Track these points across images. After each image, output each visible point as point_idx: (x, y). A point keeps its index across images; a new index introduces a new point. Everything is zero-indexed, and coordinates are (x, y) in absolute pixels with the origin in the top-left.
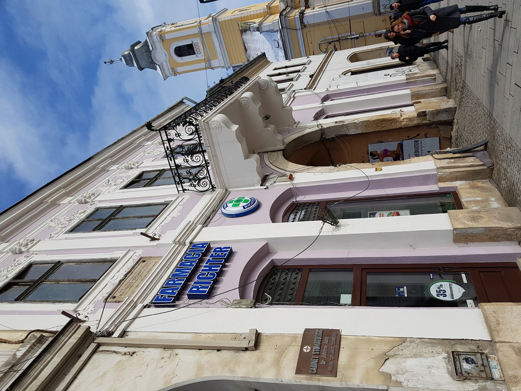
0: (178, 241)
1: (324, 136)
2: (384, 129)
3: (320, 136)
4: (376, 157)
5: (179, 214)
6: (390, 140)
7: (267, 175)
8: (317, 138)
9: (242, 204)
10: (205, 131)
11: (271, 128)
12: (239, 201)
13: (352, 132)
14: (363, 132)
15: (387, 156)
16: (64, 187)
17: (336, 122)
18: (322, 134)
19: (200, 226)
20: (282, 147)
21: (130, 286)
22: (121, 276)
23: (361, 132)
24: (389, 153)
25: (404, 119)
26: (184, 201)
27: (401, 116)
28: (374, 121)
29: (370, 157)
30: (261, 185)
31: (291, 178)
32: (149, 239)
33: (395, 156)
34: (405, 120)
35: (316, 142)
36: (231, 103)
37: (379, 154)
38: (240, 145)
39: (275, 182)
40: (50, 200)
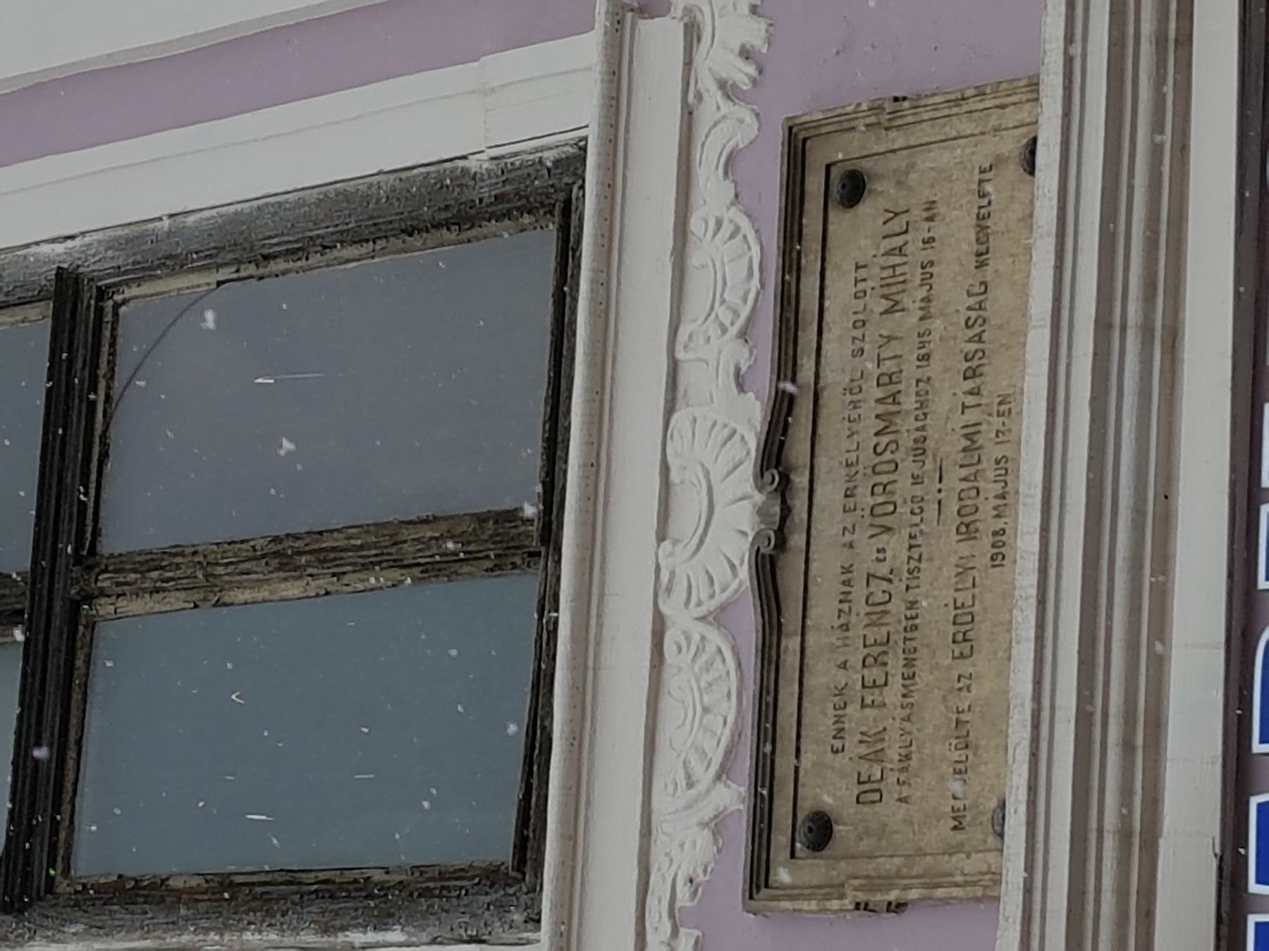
21: (892, 647)
22: (734, 516)
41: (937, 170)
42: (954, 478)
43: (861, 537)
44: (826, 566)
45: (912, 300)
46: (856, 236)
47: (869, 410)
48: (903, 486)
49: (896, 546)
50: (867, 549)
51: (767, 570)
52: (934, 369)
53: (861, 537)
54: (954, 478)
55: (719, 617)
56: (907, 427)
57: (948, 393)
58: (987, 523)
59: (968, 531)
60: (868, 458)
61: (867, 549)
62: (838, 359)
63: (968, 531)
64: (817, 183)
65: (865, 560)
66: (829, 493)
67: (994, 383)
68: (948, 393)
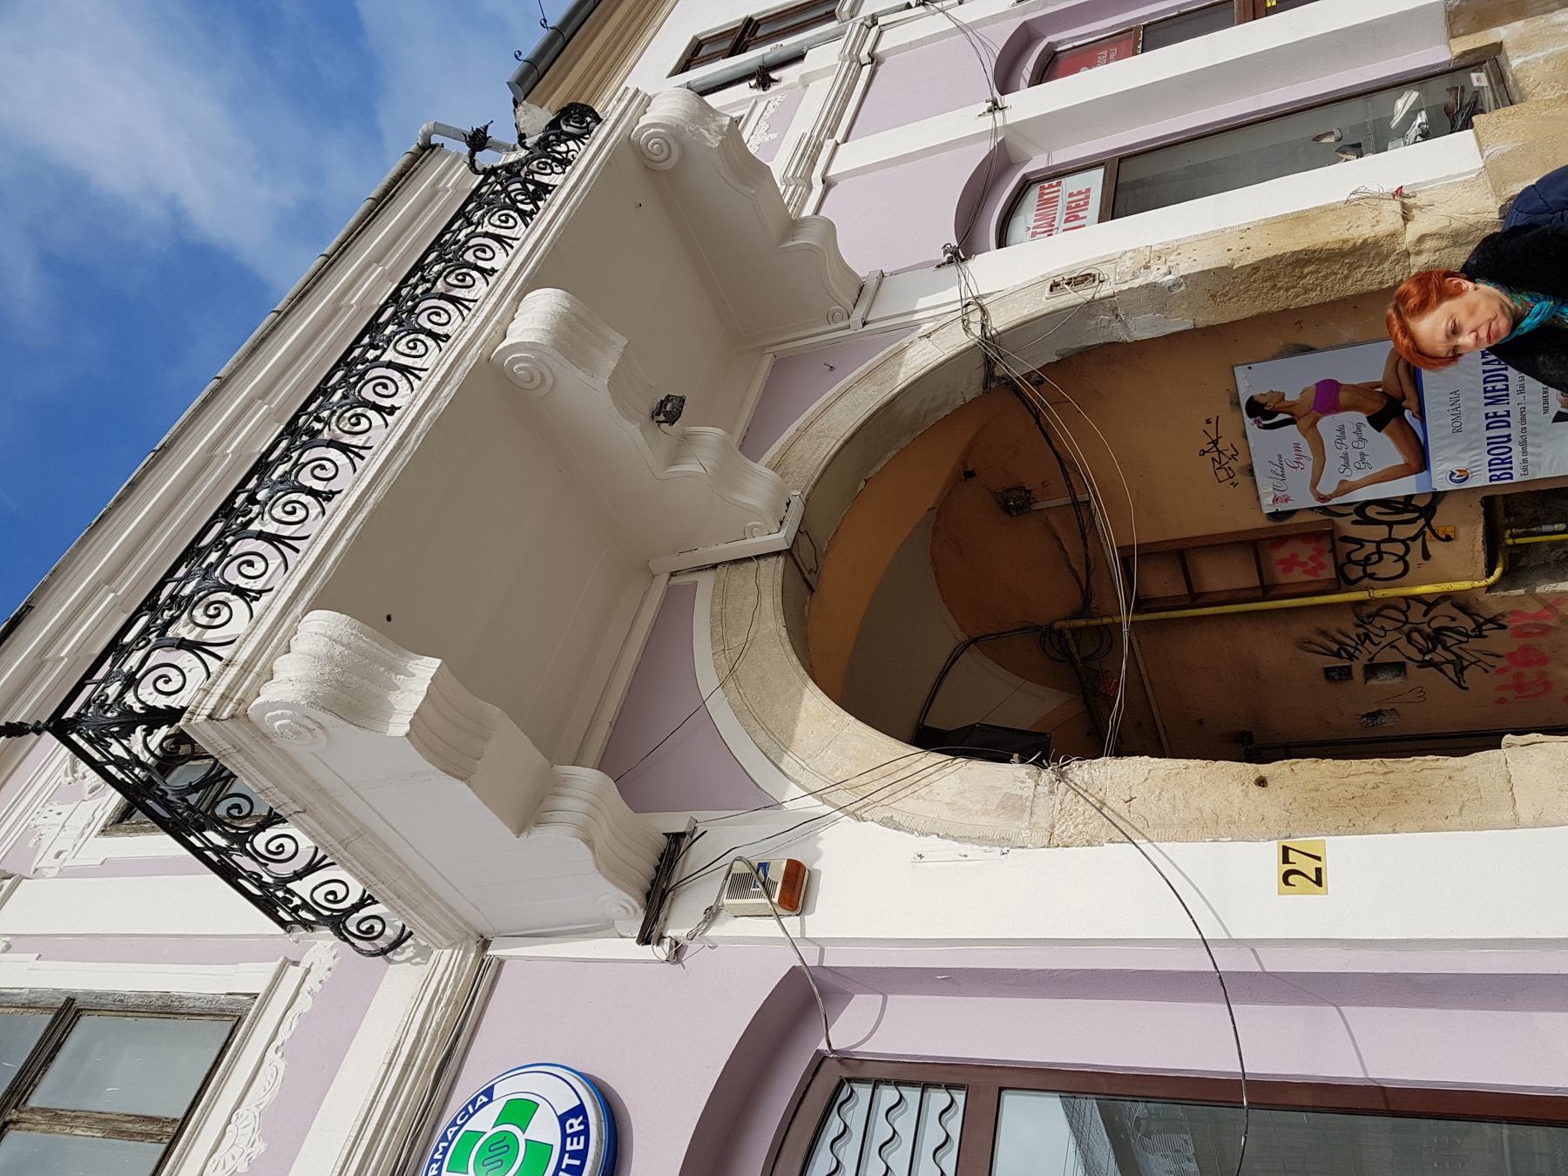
1: (1000, 371)
2: (1314, 297)
3: (979, 375)
4: (1281, 417)
5: (260, 1147)
6: (1347, 334)
7: (683, 834)
8: (970, 386)
13: (1143, 327)
14: (1203, 320)
15: (1335, 408)
18: (989, 363)
20: (779, 539)
23: (1189, 325)
24: (1344, 397)
25: (1421, 239)
26: (304, 1003)
27: (1406, 218)
28: (1255, 268)
29: (1248, 421)
30: (644, 939)
31: (795, 889)
33: (1377, 407)
34: (1429, 244)
35: (966, 406)
37: (1293, 404)
38: (464, 786)
39: (712, 914)
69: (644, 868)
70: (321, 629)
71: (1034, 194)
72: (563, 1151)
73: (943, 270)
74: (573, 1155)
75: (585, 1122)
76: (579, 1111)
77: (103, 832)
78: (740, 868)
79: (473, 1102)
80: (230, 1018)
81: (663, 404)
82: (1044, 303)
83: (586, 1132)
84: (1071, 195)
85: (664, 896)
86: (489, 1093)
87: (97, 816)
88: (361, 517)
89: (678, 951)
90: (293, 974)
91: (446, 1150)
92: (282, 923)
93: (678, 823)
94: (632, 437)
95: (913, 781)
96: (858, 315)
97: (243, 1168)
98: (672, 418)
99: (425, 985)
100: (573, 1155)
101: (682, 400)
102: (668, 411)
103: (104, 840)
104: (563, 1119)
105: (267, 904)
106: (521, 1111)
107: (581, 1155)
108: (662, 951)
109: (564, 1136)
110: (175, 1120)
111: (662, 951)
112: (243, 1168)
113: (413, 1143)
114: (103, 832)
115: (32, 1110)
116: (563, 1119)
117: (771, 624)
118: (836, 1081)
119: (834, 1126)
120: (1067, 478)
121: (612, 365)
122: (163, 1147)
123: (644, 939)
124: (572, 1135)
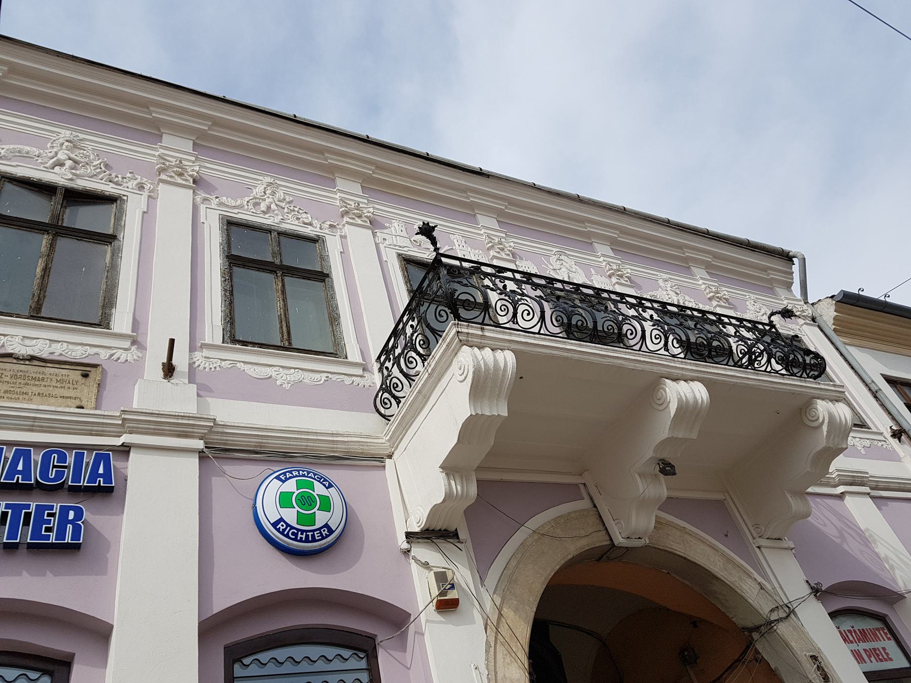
0: (124, 419)
1: (755, 635)
3: (750, 624)
8: (742, 620)
9: (290, 516)
10: (444, 346)
11: (661, 489)
12: (306, 501)
16: (379, 167)
17: (814, 658)
18: (757, 628)
19: (200, 444)
20: (619, 540)
26: (348, 380)
30: (409, 535)
32: (165, 361)
35: (730, 621)
36: (620, 368)
39: (426, 565)
40: (332, 160)
41: (87, 392)
42: (19, 390)
43: (11, 373)
44: (8, 366)
45: (58, 385)
46: (76, 375)
47: (38, 376)
48: (20, 381)
49: (8, 379)
50: (8, 374)
51: (10, 355)
52: (42, 388)
53: (11, 373)
54: (19, 390)
55: (3, 346)
56: (32, 382)
57: (36, 390)
58: (6, 395)
59: (6, 392)
60: (27, 375)
61: (8, 374)
62: (50, 371)
63: (6, 392)
64: (86, 369)
65: (5, 373)
66: (23, 367)
67: (35, 398)
68: (36, 390)
69: (439, 525)
70: (507, 359)
71: (878, 624)
72: (313, 531)
73: (806, 585)
74: (313, 536)
75: (327, 536)
76: (331, 531)
77: (399, 255)
78: (449, 575)
79: (325, 480)
80: (336, 352)
81: (669, 464)
82: (803, 655)
83: (323, 538)
84: (884, 649)
85: (428, 538)
86: (330, 486)
87: (406, 249)
88: (566, 354)
89: (407, 552)
90: (359, 371)
91: (303, 476)
92: (379, 357)
93: (463, 534)
94: (648, 453)
95: (511, 652)
96: (763, 542)
97: (278, 383)
98: (662, 471)
99: (368, 437)
100: (313, 536)
101: (674, 474)
102: (667, 469)
103: (395, 256)
104: (326, 526)
105: (386, 351)
106: (326, 505)
107: (314, 540)
108: (405, 546)
109: (319, 529)
110: (290, 344)
111: (405, 546)
112: (278, 383)
113: (303, 457)
114: (399, 255)
115: (283, 280)
116: (326, 526)
117: (573, 548)
118: (366, 648)
119: (346, 653)
120: (726, 670)
121: (680, 436)
122: (279, 344)
123: (409, 535)
124: (321, 533)
